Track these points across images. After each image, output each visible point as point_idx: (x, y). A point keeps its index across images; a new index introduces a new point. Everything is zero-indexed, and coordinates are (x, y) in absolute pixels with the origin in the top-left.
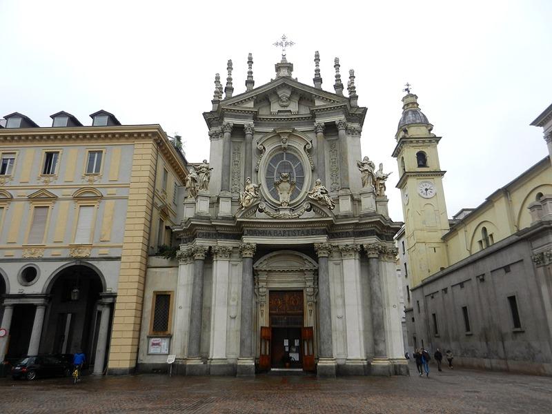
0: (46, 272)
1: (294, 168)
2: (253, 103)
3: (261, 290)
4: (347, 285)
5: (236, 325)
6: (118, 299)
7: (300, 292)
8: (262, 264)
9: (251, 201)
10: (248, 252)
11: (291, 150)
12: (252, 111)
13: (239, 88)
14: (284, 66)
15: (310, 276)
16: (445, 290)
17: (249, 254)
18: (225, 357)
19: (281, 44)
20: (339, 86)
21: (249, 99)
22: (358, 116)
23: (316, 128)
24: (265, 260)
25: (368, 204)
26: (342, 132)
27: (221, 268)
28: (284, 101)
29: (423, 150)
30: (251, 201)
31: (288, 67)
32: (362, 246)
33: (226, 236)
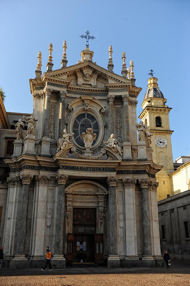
2: (66, 76)
3: (68, 207)
4: (127, 206)
7: (94, 210)
8: (70, 189)
9: (67, 146)
11: (91, 111)
12: (66, 82)
13: (58, 66)
15: (102, 199)
16: (172, 210)
17: (63, 182)
18: (42, 255)
19: (86, 37)
21: (64, 73)
22: (134, 93)
23: (109, 98)
24: (72, 186)
25: (142, 153)
26: (126, 103)
27: (42, 191)
28: (87, 78)
29: (161, 116)
30: (67, 146)
31: (91, 54)
32: (137, 180)
33: (46, 169)
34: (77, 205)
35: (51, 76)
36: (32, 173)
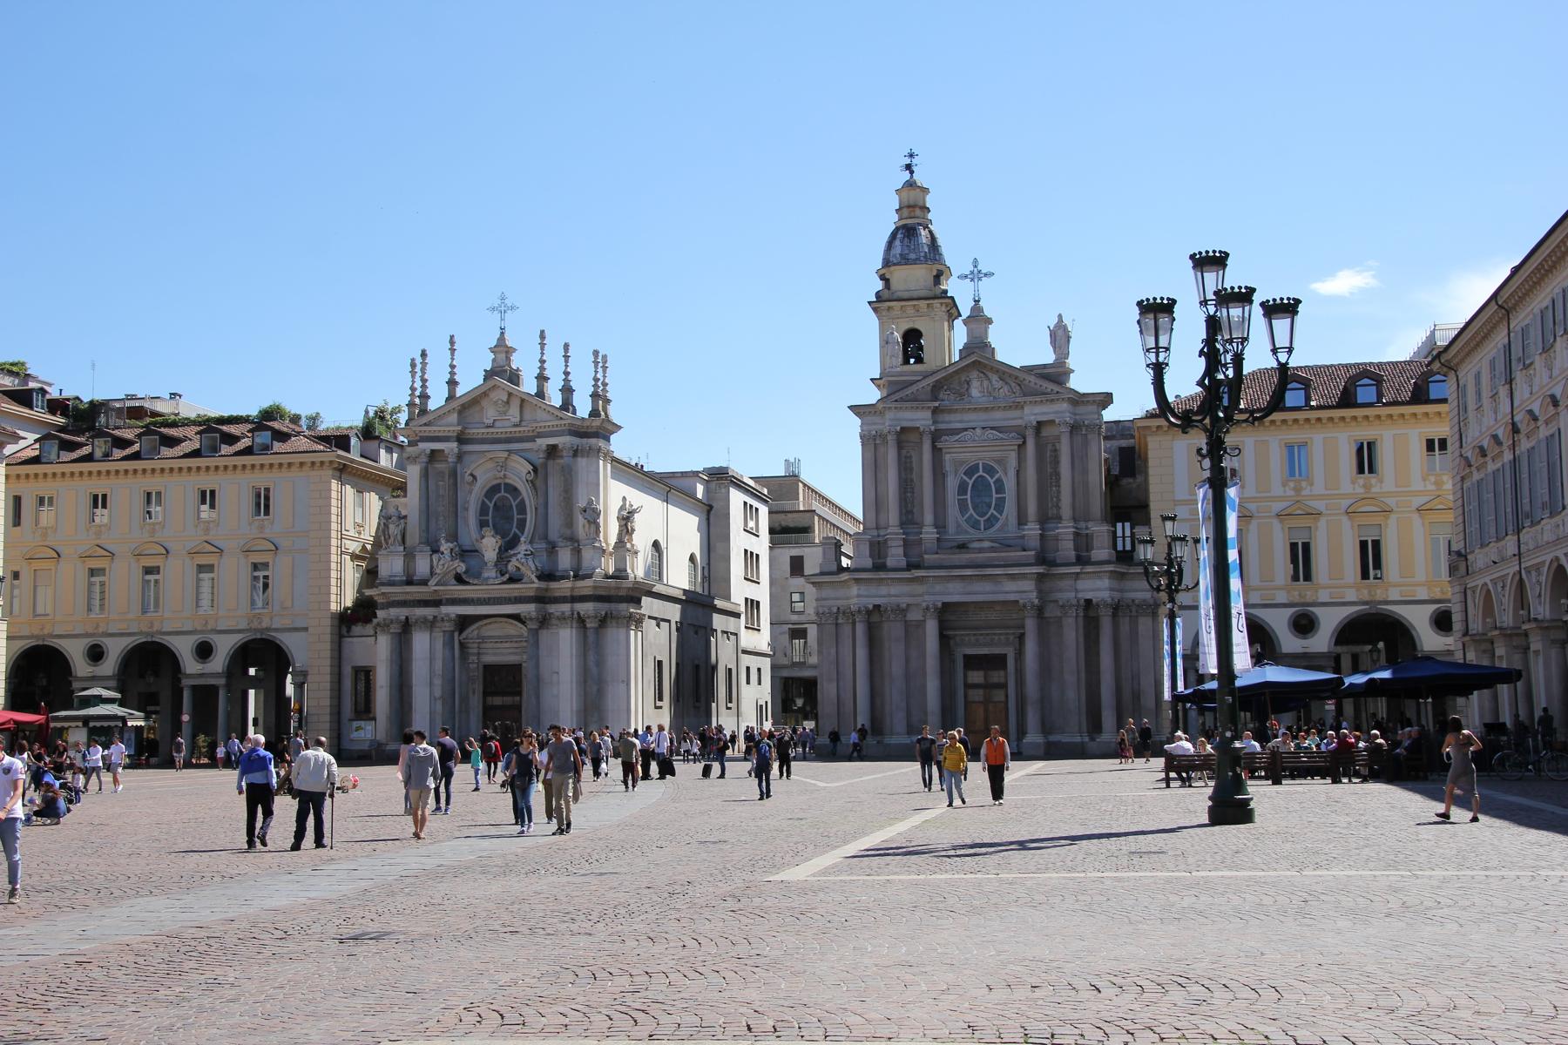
0: (224, 646)
5: (439, 706)
6: (310, 678)
14: (502, 349)
17: (448, 626)
20: (567, 391)
27: (421, 642)
29: (919, 325)
34: (489, 659)
36: (402, 613)
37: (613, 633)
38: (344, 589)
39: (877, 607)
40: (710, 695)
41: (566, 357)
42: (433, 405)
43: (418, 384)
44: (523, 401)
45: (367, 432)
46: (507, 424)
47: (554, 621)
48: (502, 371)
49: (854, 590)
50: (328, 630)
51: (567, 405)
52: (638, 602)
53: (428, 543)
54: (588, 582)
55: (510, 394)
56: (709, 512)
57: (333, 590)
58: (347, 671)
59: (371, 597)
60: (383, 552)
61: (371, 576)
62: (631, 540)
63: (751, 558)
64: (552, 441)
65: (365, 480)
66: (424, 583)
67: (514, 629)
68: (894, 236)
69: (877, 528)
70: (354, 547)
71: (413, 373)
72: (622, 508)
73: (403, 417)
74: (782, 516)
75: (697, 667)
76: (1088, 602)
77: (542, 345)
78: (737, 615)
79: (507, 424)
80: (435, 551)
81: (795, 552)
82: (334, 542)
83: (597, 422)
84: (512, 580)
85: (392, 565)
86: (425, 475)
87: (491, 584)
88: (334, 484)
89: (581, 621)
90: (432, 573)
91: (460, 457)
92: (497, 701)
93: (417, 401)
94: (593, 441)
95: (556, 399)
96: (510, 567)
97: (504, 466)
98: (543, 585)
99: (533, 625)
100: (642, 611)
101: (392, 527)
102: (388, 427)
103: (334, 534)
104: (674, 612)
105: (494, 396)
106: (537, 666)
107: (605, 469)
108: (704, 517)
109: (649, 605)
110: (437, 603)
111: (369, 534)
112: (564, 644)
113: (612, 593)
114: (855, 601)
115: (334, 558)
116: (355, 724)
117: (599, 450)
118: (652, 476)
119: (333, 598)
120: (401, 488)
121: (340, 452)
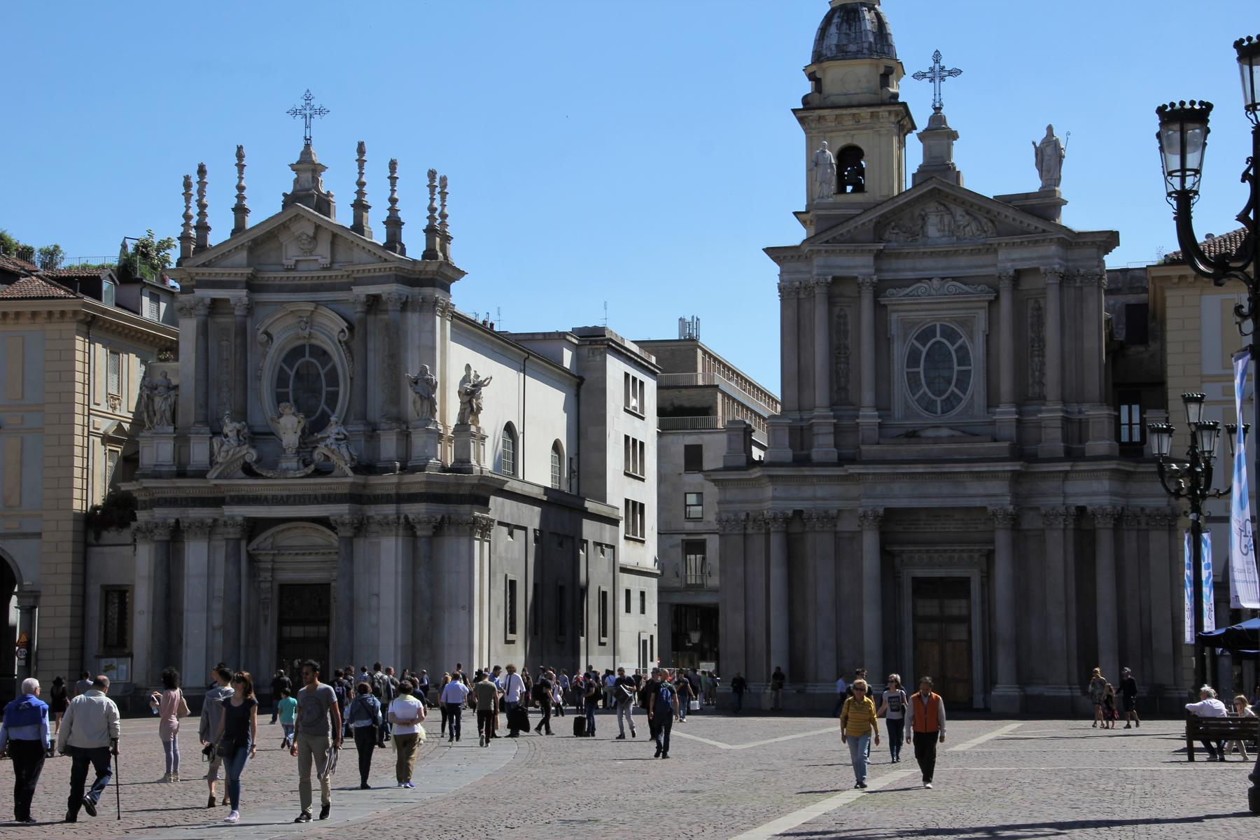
1: (322, 373)
2: (244, 254)
3: (262, 585)
5: (219, 638)
6: (42, 600)
9: (231, 453)
10: (231, 530)
14: (307, 166)
17: (233, 533)
20: (394, 224)
27: (196, 553)
29: (861, 140)
30: (231, 453)
32: (406, 518)
34: (288, 576)
35: (204, 265)
37: (451, 544)
38: (92, 483)
39: (798, 513)
40: (577, 626)
41: (393, 180)
42: (213, 239)
43: (194, 211)
44: (334, 236)
45: (125, 273)
46: (313, 266)
47: (374, 527)
48: (307, 195)
49: (769, 491)
50: (70, 536)
51: (394, 240)
52: (484, 503)
53: (206, 422)
54: (419, 477)
55: (318, 227)
56: (579, 386)
57: (77, 483)
58: (95, 591)
59: (129, 493)
60: (145, 433)
61: (128, 465)
62: (476, 422)
63: (633, 447)
64: (373, 290)
65: (122, 338)
66: (201, 474)
67: (320, 537)
68: (828, 20)
69: (800, 410)
70: (105, 426)
71: (187, 196)
72: (465, 380)
73: (174, 255)
74: (674, 393)
75: (562, 589)
76: (1081, 510)
77: (361, 163)
78: (615, 522)
79: (313, 266)
80: (217, 432)
81: (691, 440)
82: (78, 419)
83: (432, 266)
84: (319, 473)
85: (158, 451)
86: (203, 332)
87: (292, 478)
88: (80, 343)
89: (410, 527)
90: (212, 462)
91: (250, 309)
92: (297, 631)
93: (193, 233)
94: (428, 291)
95: (379, 235)
96: (317, 456)
97: (310, 322)
98: (360, 479)
99: (346, 532)
100: (490, 515)
101: (157, 400)
102: (154, 267)
103: (78, 409)
104: (531, 517)
105: (296, 228)
106: (351, 586)
107: (442, 327)
108: (573, 392)
109: (499, 508)
110: (218, 502)
111: (127, 409)
112: (387, 556)
113: (451, 490)
114: (769, 504)
115: (78, 440)
116: (104, 662)
117: (436, 302)
118: (504, 337)
119: (77, 494)
120: (170, 349)
121: (88, 300)
